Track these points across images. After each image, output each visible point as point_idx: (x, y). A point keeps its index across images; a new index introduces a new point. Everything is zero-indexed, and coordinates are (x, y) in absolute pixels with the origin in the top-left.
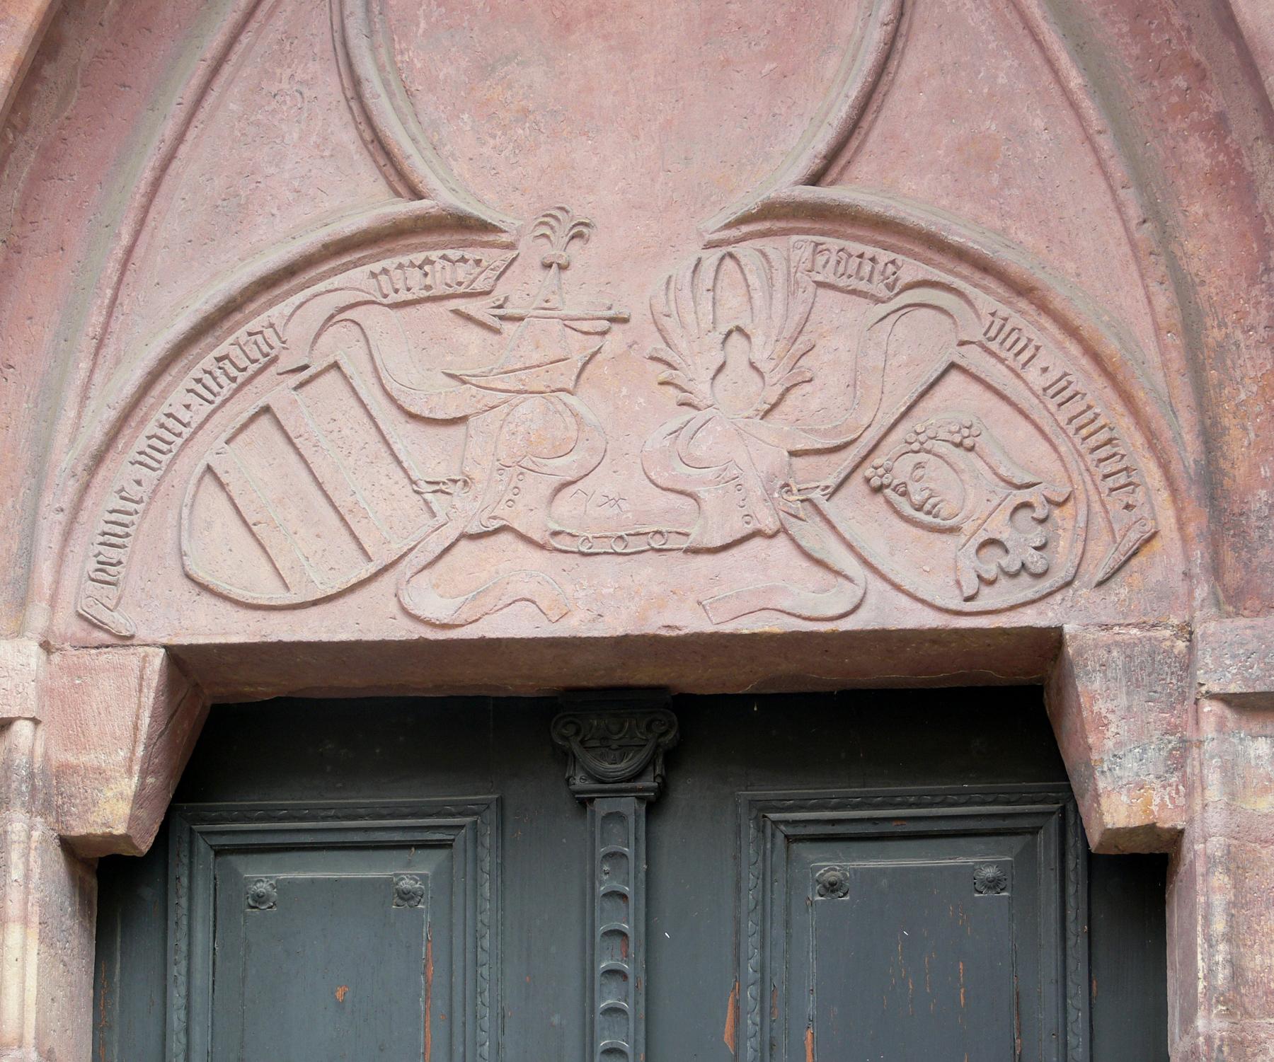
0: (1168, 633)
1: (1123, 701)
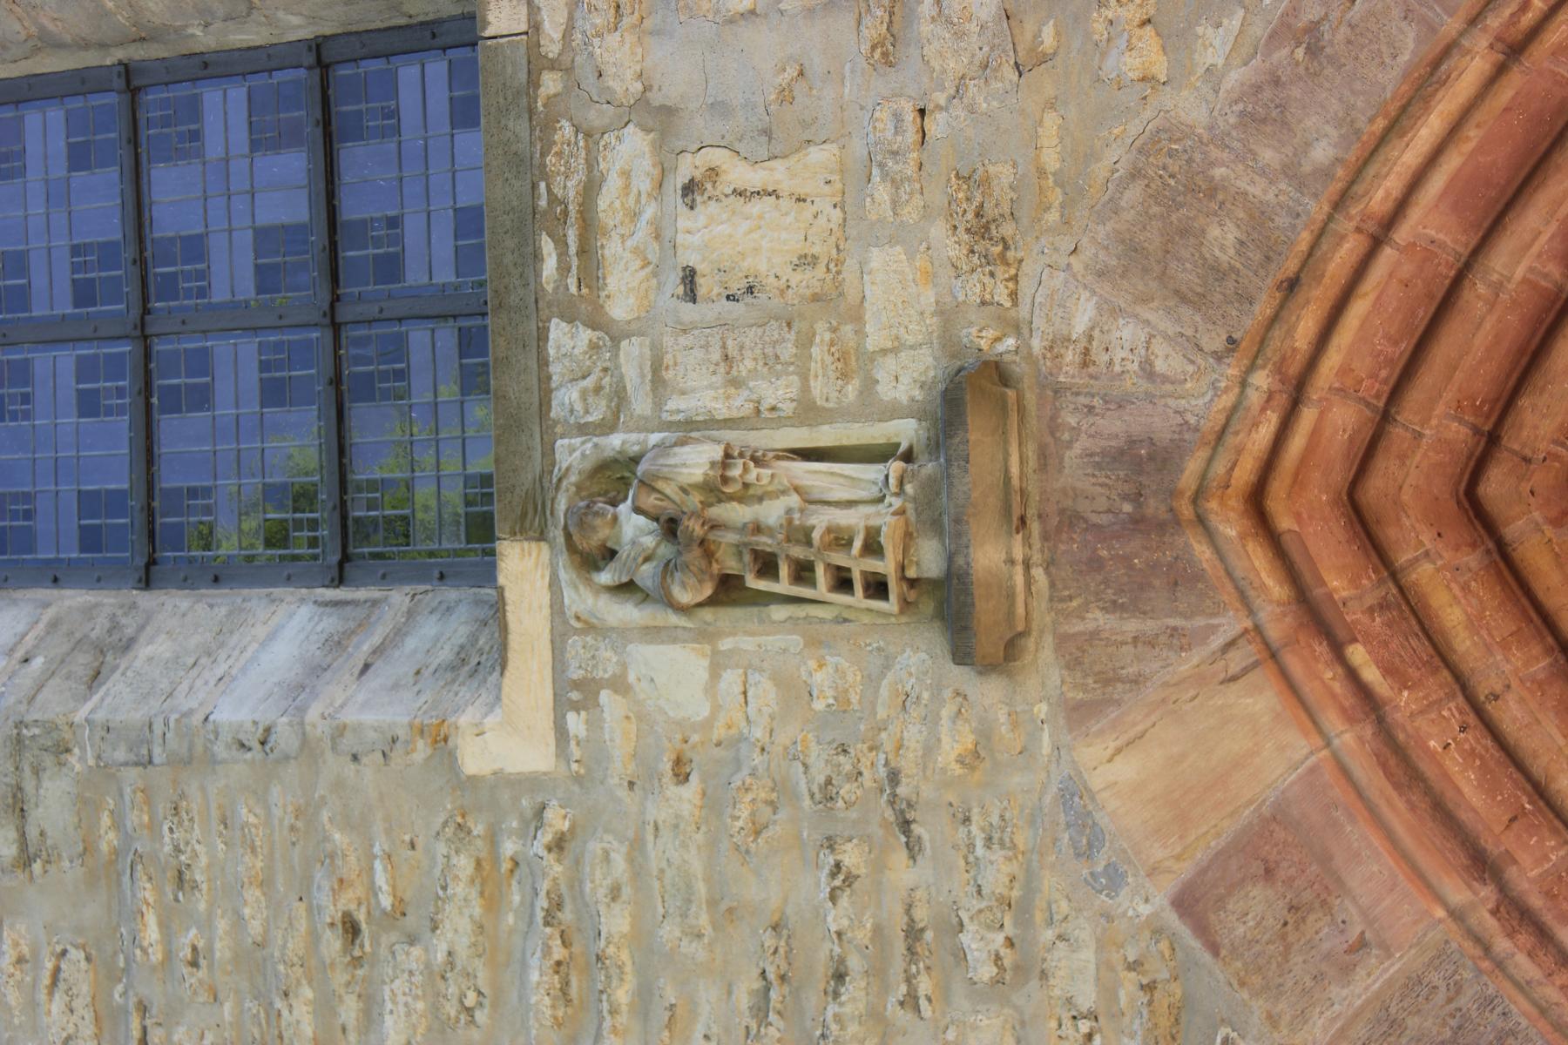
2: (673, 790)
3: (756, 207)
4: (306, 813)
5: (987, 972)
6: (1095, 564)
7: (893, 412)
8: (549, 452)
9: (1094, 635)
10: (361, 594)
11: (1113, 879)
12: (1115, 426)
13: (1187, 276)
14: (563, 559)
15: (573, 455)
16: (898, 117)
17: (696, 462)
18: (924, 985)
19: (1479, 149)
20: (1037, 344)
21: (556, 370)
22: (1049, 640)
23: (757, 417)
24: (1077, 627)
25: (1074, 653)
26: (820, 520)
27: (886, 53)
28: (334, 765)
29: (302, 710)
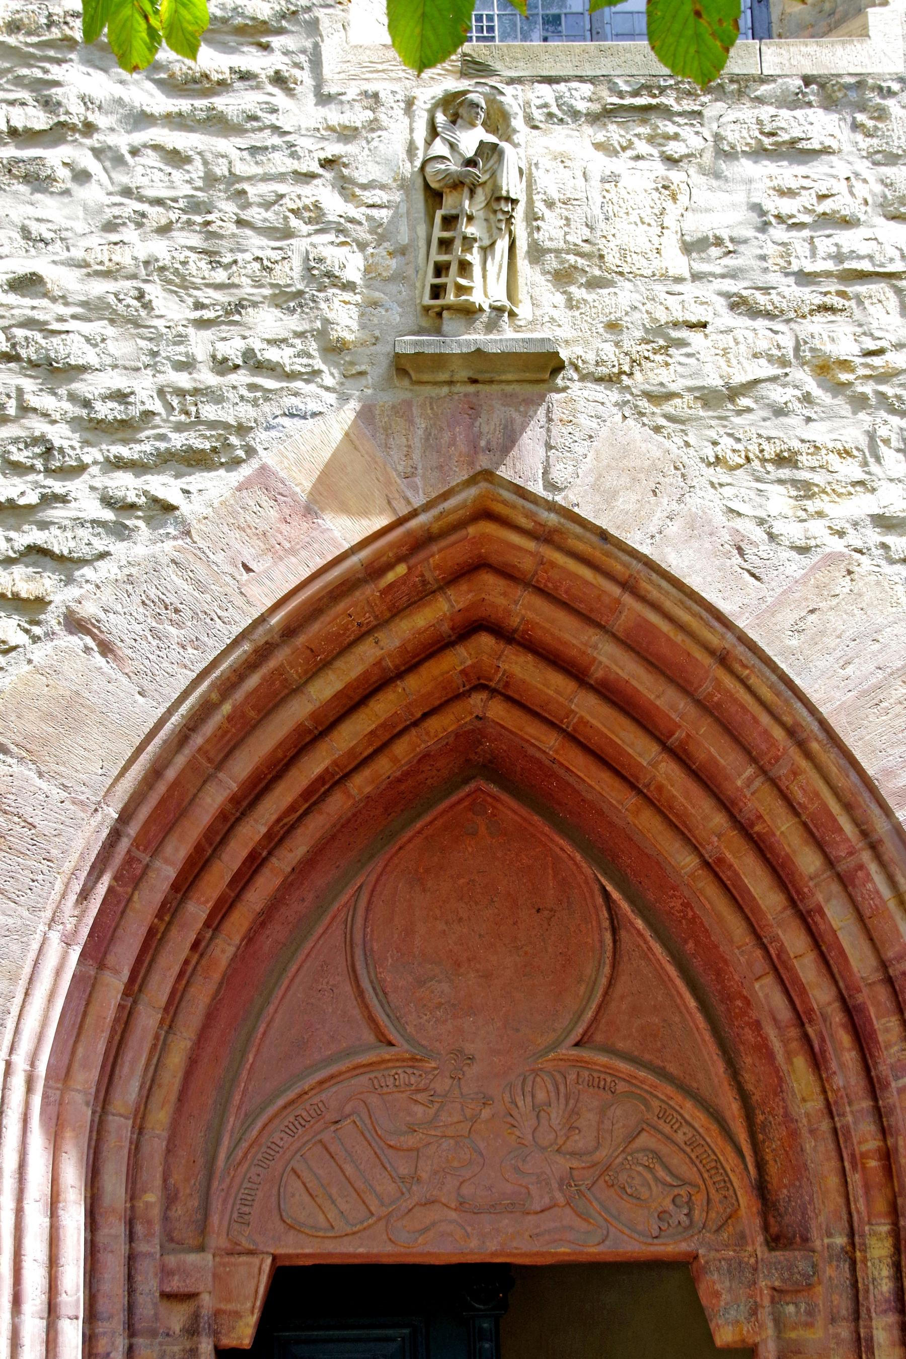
0: (747, 1254)
1: (727, 1284)
9: (411, 422)
13: (611, 481)
19: (669, 639)
24: (416, 411)
25: (402, 411)
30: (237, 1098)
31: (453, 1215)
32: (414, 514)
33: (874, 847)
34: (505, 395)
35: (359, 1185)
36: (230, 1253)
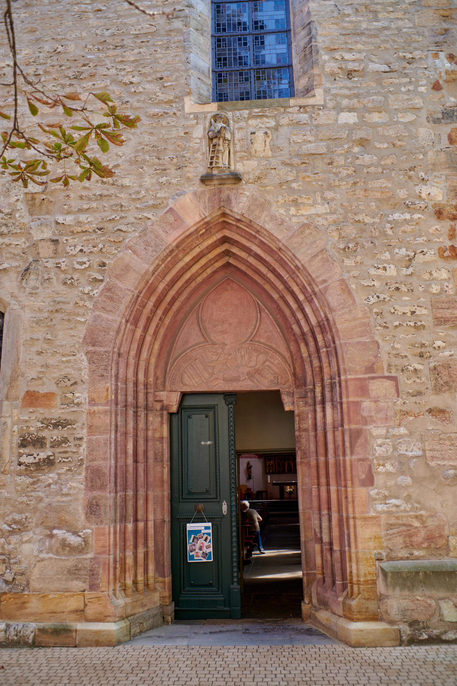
2: (183, 132)
3: (263, 144)
4: (178, 70)
5: (161, 181)
6: (214, 195)
7: (235, 166)
8: (230, 111)
10: (211, 75)
11: (174, 199)
12: (233, 198)
14: (215, 113)
15: (230, 115)
16: (274, 165)
17: (228, 136)
18: (158, 172)
20: (244, 186)
21: (241, 112)
22: (204, 189)
23: (234, 144)
24: (206, 193)
25: (203, 193)
26: (220, 155)
27: (284, 163)
28: (185, 75)
29: (193, 69)
30: (172, 355)
31: (222, 382)
32: (206, 217)
33: (315, 294)
34: (227, 188)
35: (200, 375)
36: (170, 391)
